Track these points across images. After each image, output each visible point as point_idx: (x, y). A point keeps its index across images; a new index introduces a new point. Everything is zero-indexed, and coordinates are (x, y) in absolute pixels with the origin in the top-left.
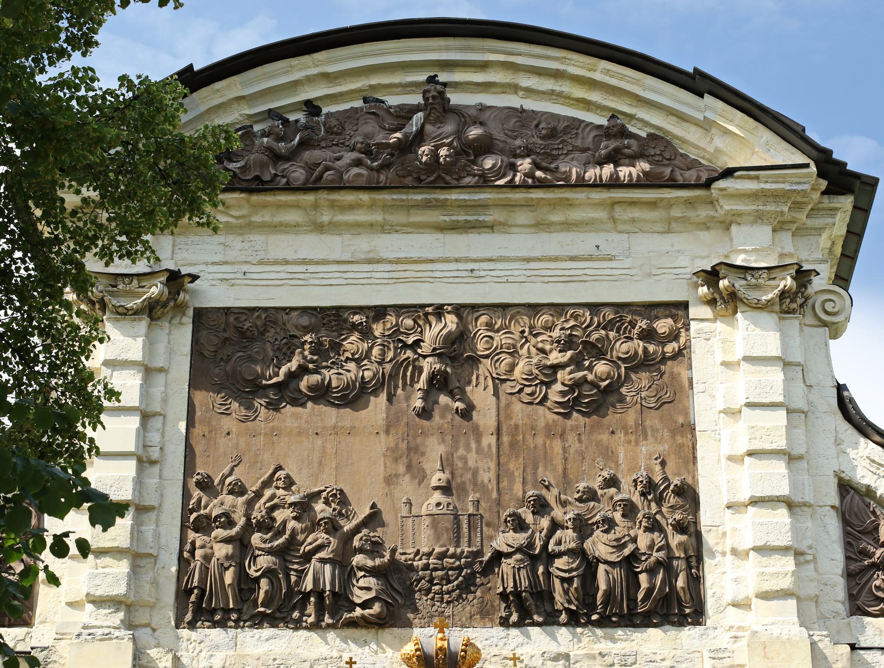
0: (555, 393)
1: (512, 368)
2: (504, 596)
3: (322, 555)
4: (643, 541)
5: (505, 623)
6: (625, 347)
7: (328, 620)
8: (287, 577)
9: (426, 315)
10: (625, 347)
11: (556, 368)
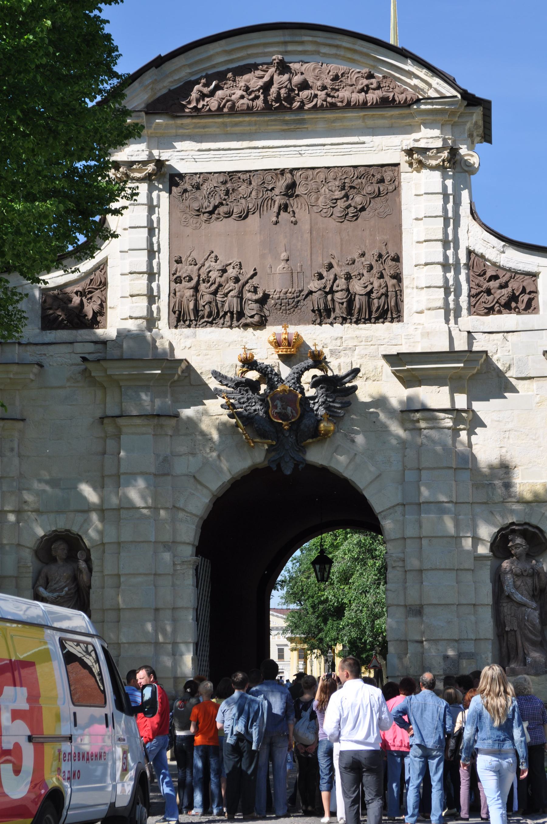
0: (338, 212)
1: (317, 199)
2: (313, 311)
3: (231, 294)
4: (376, 285)
5: (314, 323)
6: (370, 188)
7: (235, 323)
8: (217, 305)
9: (276, 174)
10: (370, 188)
11: (337, 199)
